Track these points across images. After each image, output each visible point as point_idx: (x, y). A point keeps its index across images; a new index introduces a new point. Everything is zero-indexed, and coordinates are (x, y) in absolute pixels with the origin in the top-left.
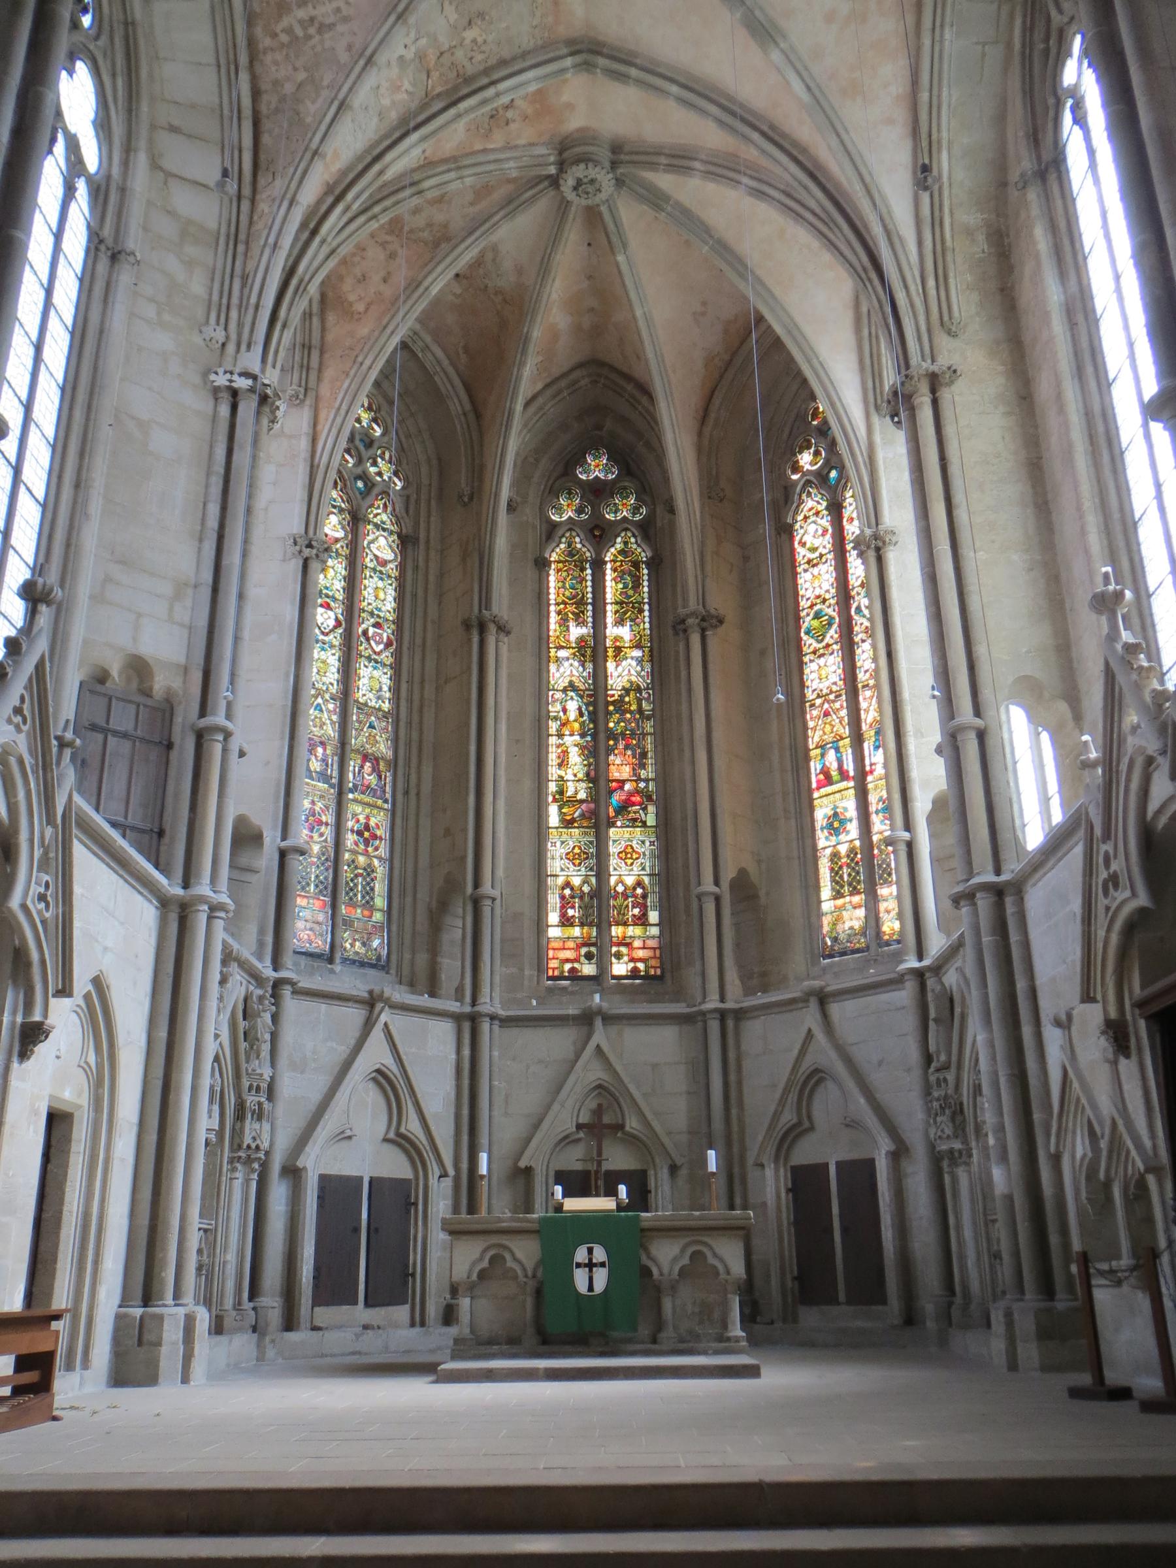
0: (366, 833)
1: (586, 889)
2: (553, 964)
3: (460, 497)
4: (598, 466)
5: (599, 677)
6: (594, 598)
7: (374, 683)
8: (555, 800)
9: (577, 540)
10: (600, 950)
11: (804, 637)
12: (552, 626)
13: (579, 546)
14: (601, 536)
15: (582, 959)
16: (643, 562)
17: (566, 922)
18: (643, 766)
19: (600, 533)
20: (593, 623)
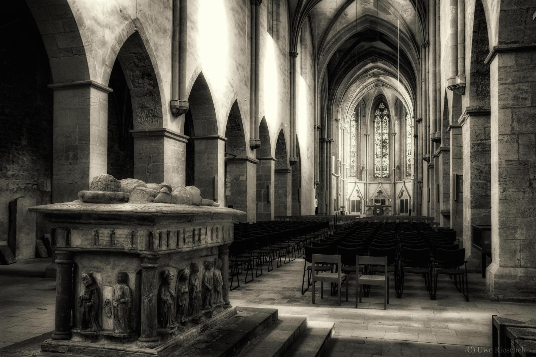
0: (353, 161)
7: (354, 142)
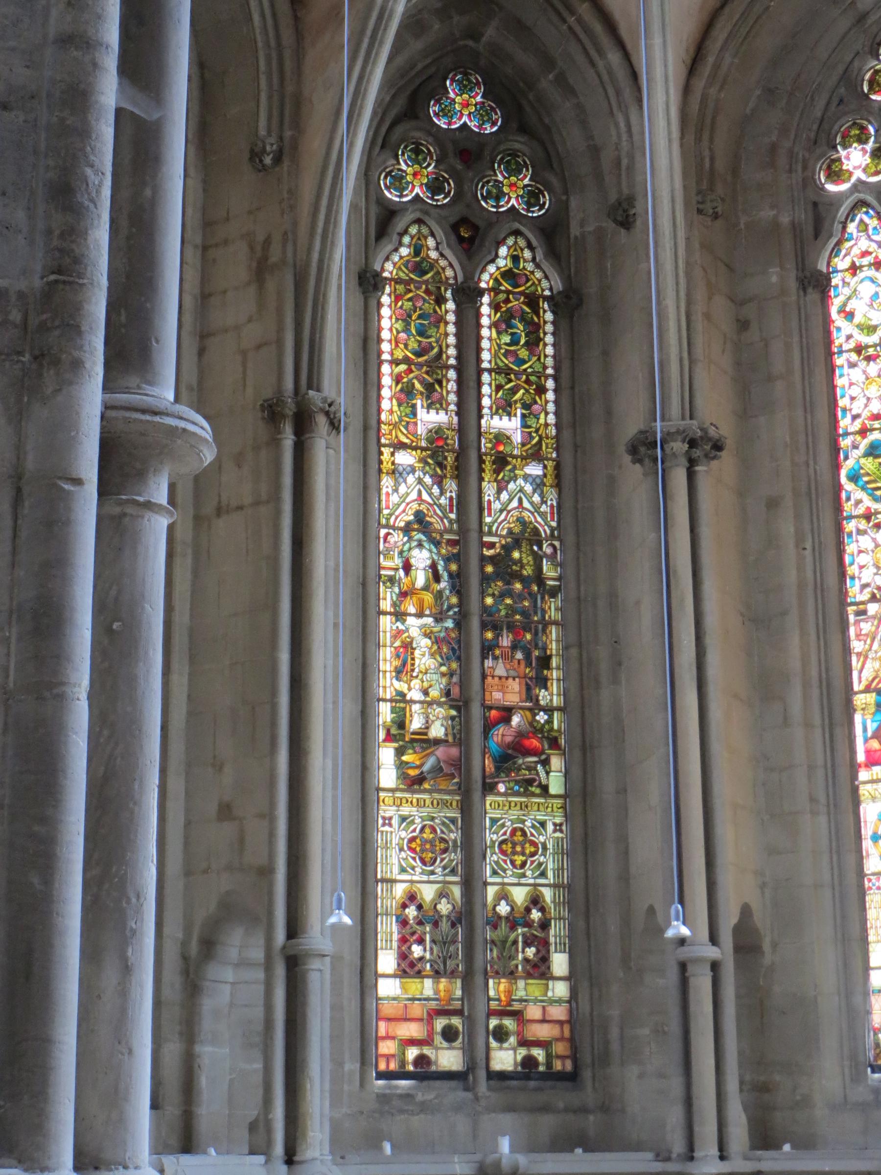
1: (444, 908)
2: (387, 1047)
3: (256, 155)
4: (466, 105)
5: (468, 506)
6: (458, 358)
8: (389, 738)
9: (431, 242)
10: (470, 1022)
11: (848, 486)
12: (385, 405)
13: (433, 255)
14: (471, 240)
15: (438, 1039)
16: (545, 298)
17: (408, 968)
18: (544, 683)
19: (471, 236)
20: (459, 405)
